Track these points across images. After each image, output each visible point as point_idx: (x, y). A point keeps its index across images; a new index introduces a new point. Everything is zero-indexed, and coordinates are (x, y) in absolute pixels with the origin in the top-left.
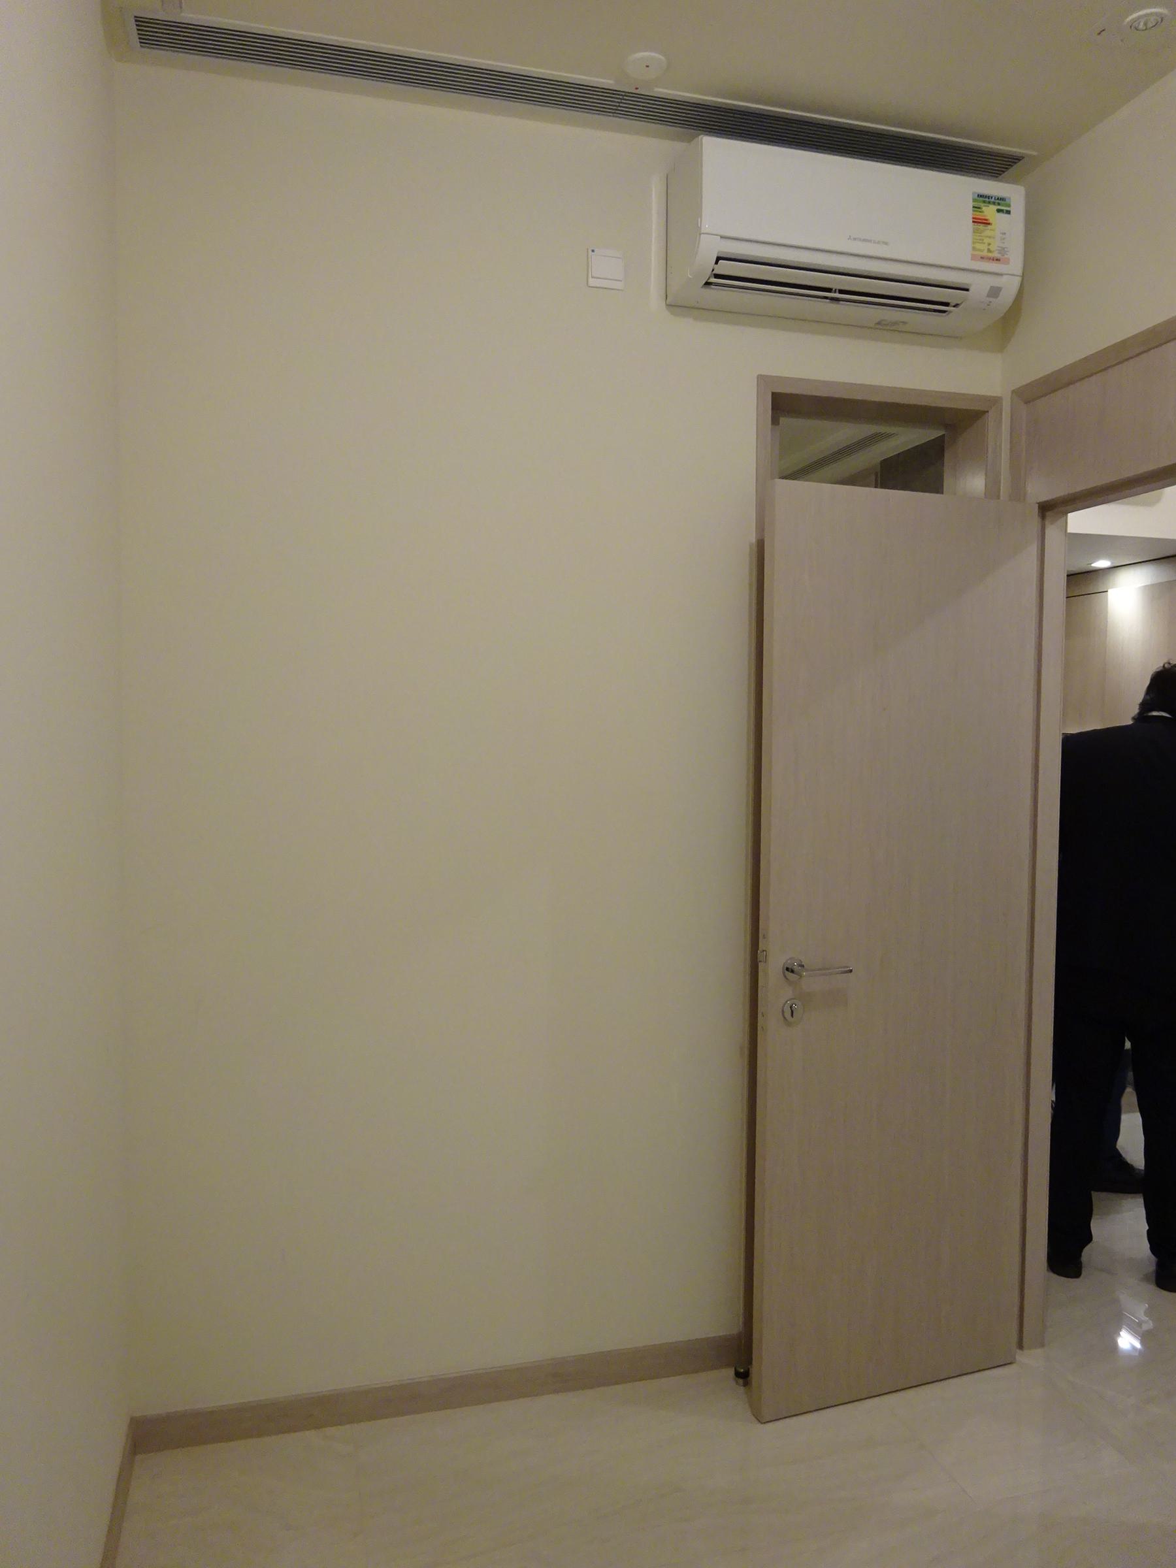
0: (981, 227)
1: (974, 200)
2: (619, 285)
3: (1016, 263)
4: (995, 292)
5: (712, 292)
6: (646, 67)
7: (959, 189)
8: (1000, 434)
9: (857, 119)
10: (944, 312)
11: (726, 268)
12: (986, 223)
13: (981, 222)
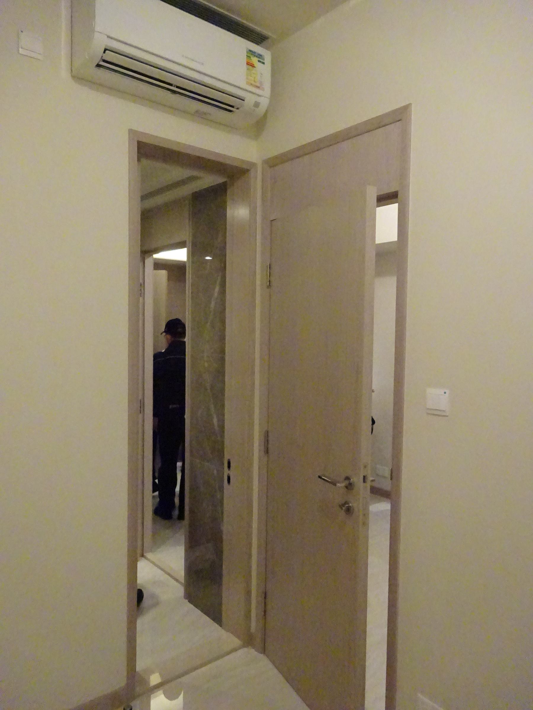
0: (251, 67)
1: (247, 53)
2: (40, 57)
3: (267, 91)
4: (257, 105)
5: (101, 71)
7: (240, 45)
8: (257, 182)
10: (230, 111)
11: (110, 56)
12: (253, 66)
13: (250, 64)
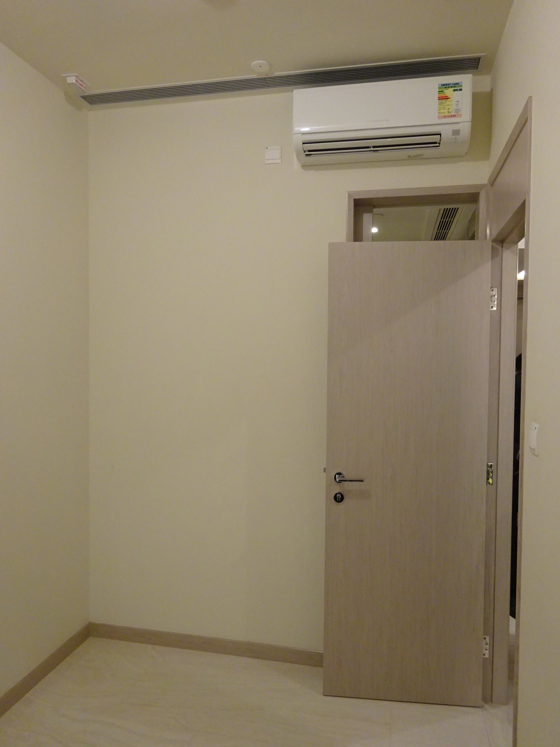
1: (439, 88)
2: (279, 161)
3: (466, 115)
4: (456, 132)
6: (258, 67)
7: (432, 83)
9: (365, 63)
12: (447, 98)
13: (443, 98)
